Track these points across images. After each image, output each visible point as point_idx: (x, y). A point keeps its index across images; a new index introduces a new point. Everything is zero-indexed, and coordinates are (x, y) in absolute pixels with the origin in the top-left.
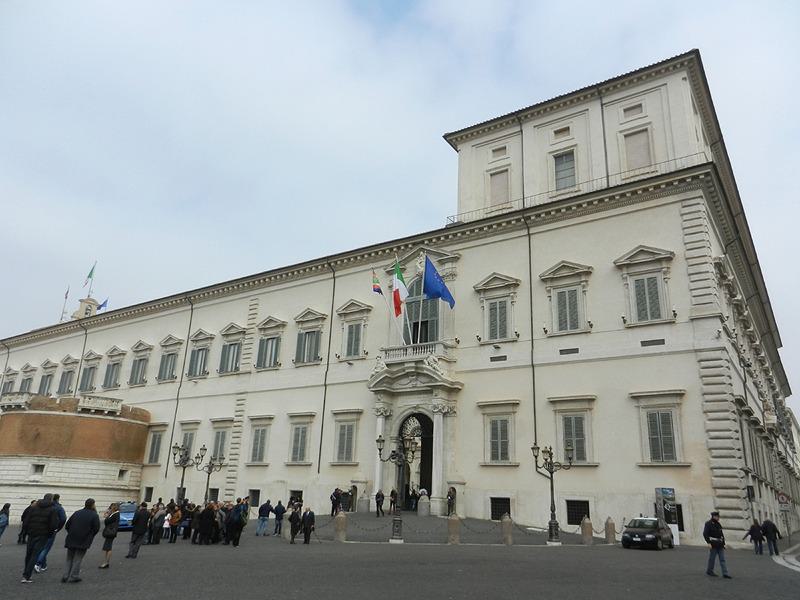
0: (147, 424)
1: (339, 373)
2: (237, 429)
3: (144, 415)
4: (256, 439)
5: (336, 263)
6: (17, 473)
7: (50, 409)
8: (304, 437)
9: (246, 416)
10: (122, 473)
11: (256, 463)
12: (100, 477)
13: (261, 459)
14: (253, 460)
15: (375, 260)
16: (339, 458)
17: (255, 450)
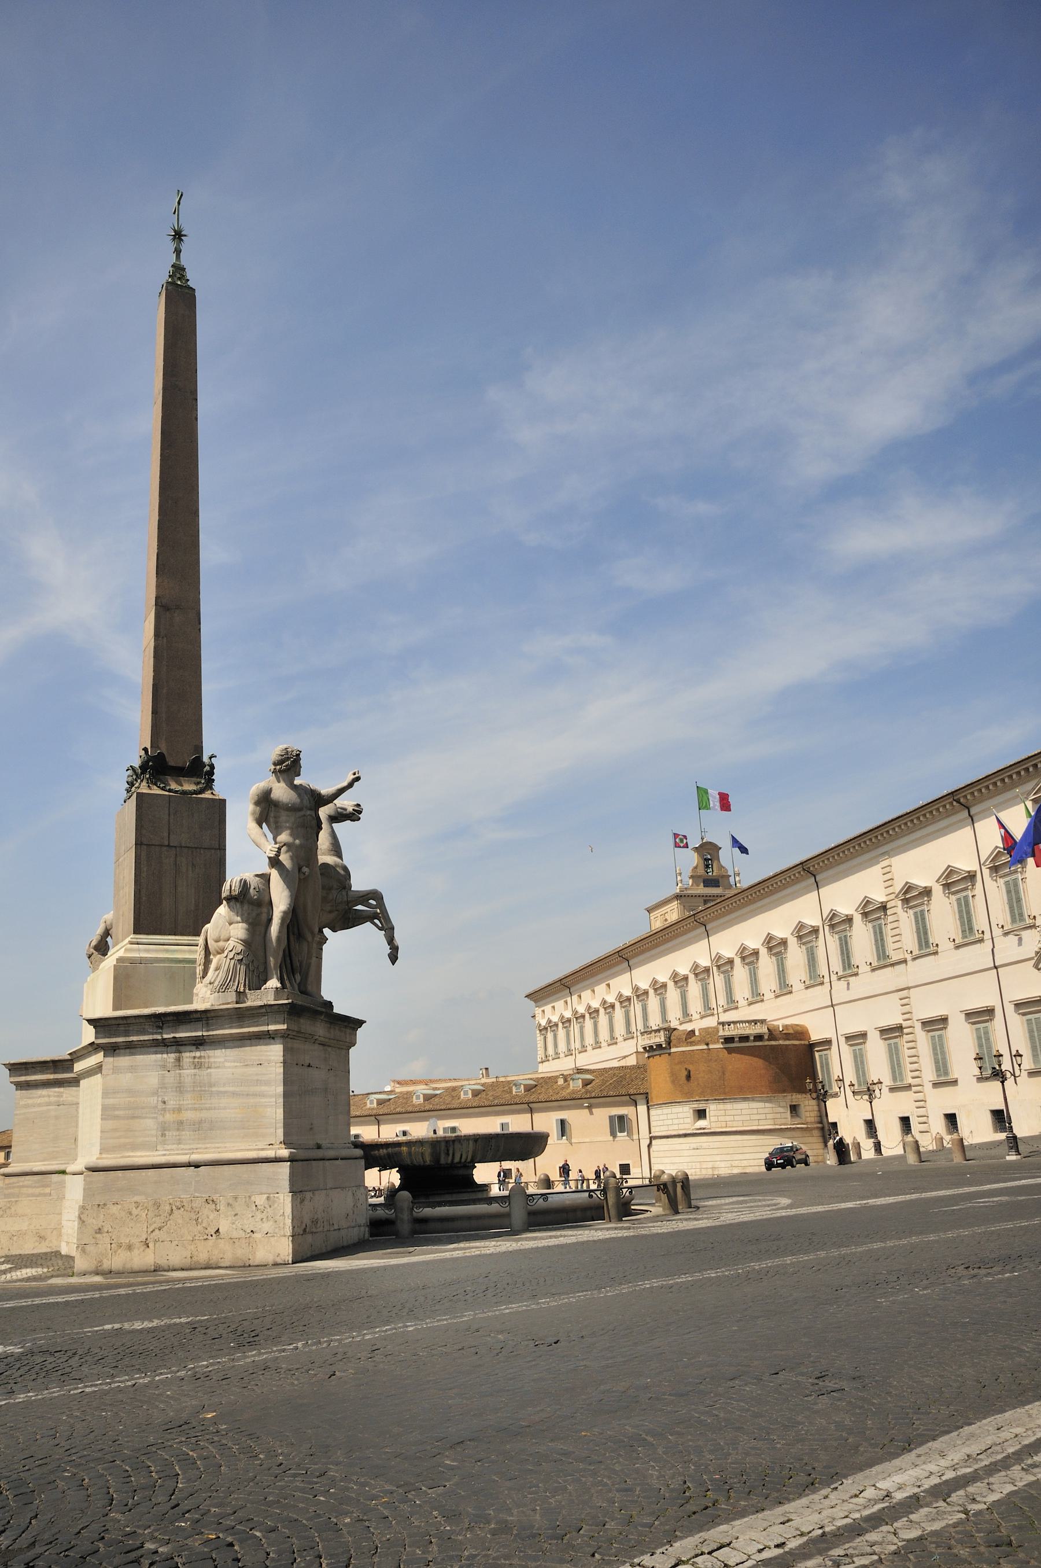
0: (806, 1043)
1: (1008, 949)
2: (910, 1037)
3: (800, 1033)
4: (934, 1049)
5: (965, 797)
6: (681, 1121)
7: (692, 1044)
8: (988, 1039)
9: (915, 1019)
10: (794, 1109)
11: (943, 1079)
12: (769, 1116)
13: (946, 1073)
14: (938, 1076)
15: (1014, 786)
16: (1034, 1062)
17: (937, 1062)
